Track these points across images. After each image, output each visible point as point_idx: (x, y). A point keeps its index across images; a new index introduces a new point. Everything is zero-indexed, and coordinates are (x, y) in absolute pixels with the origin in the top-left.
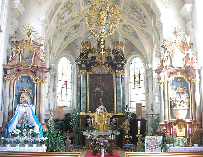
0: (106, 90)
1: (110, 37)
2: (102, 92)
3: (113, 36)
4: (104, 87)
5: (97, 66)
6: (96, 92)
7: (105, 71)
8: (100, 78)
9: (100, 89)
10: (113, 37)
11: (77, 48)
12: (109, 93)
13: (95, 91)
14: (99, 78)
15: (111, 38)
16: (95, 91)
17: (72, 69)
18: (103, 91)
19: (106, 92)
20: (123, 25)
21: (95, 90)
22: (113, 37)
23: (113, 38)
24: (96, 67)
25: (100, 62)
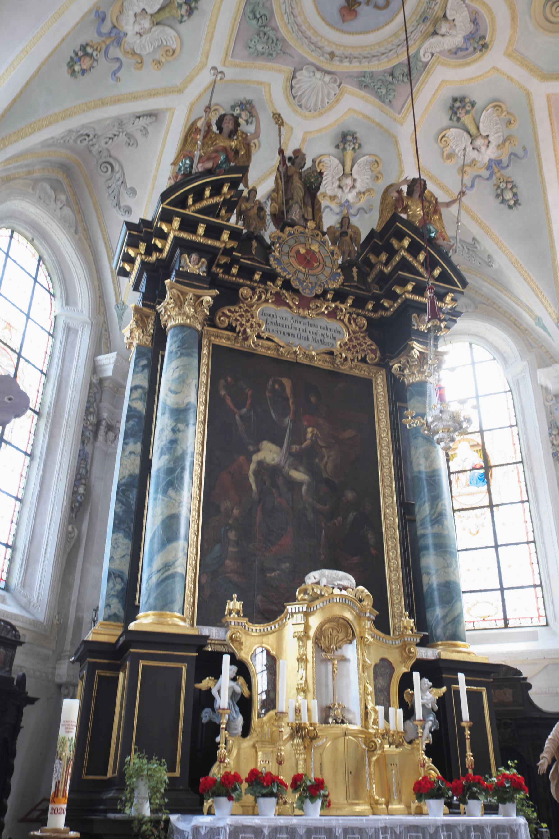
0: (330, 467)
1: (337, 183)
2: (299, 475)
3: (358, 184)
4: (314, 443)
5: (279, 301)
6: (257, 474)
7: (322, 342)
8: (287, 383)
9: (290, 454)
10: (354, 192)
11: (118, 205)
12: (350, 495)
13: (253, 466)
14: (282, 386)
15: (339, 192)
16: (250, 461)
17: (60, 334)
18: (312, 471)
19: (328, 481)
20: (455, 100)
21: (256, 458)
22: (354, 192)
23: (351, 197)
24: (271, 307)
25: (301, 276)
